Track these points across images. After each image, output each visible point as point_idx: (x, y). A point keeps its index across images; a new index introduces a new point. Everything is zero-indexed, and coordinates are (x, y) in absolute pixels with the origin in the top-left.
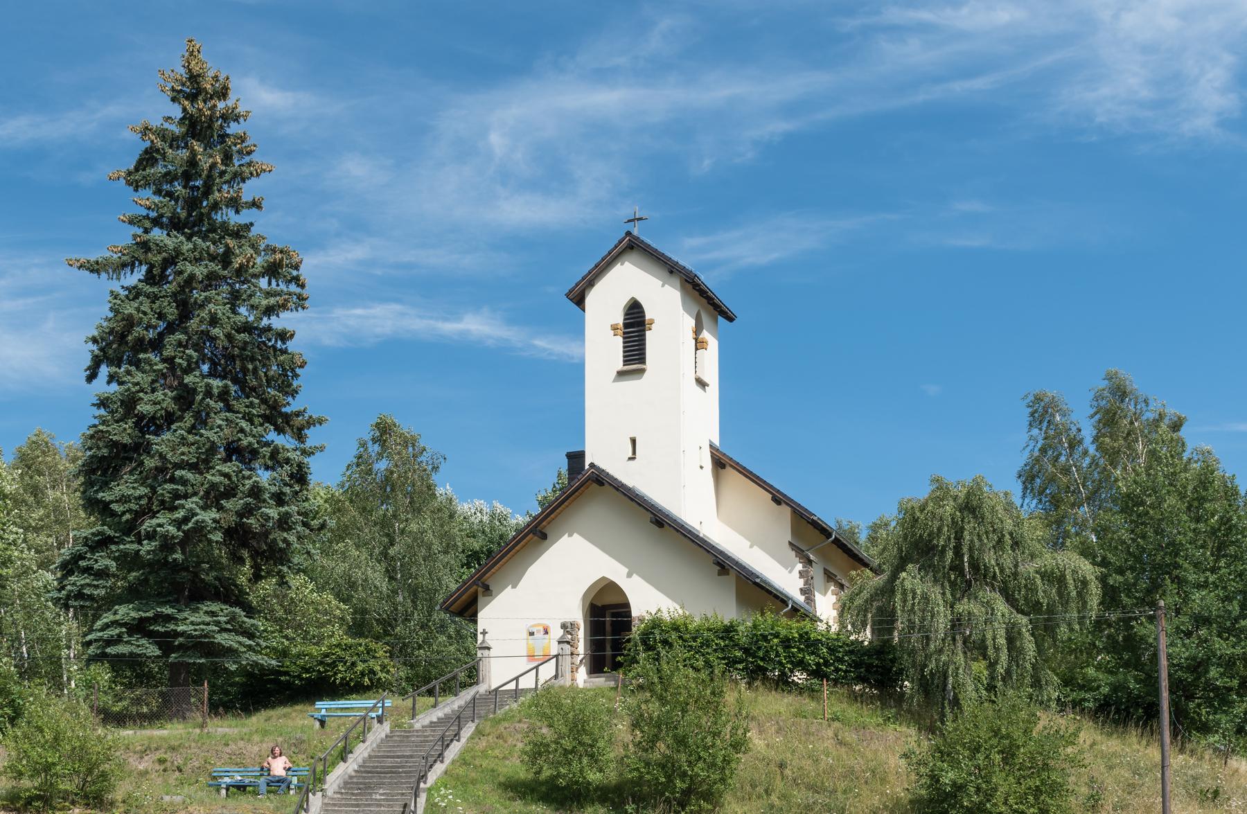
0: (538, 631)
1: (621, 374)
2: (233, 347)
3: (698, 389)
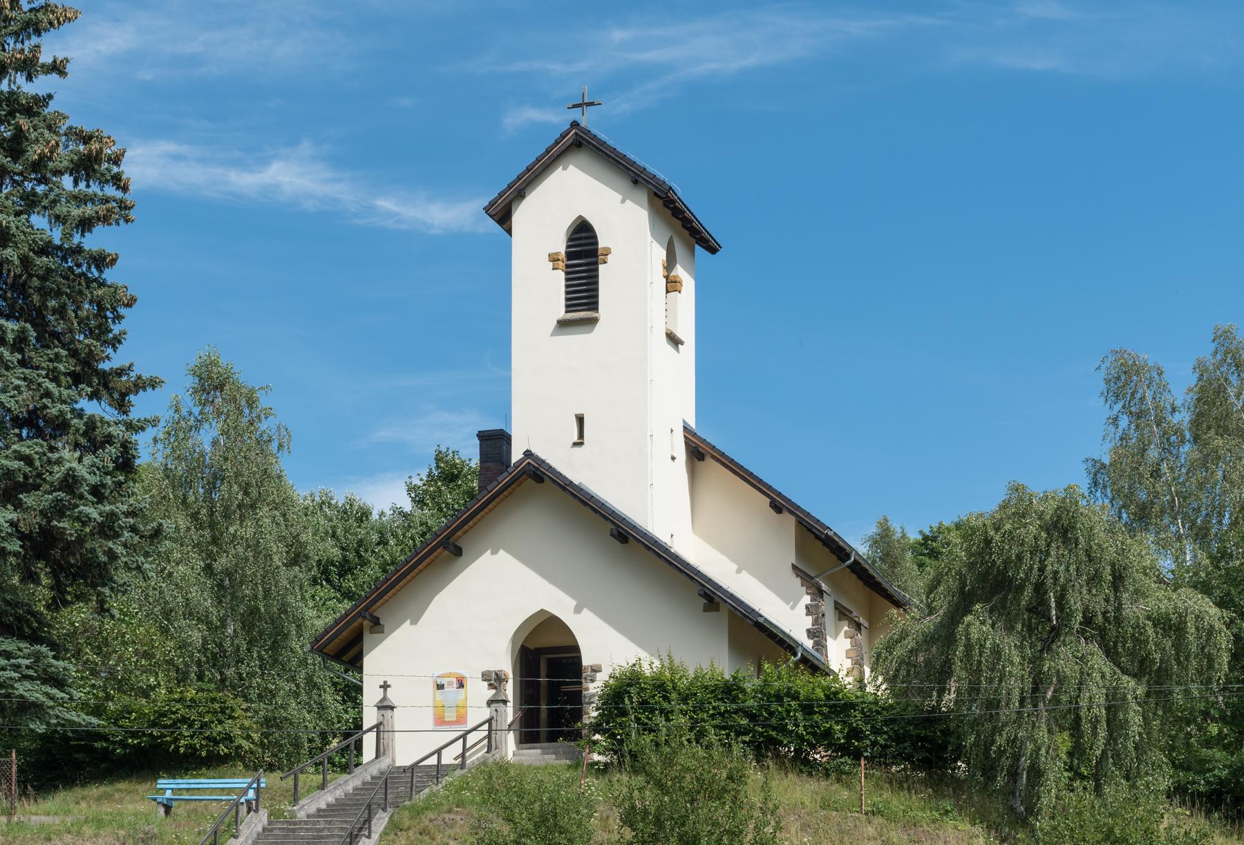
0: (450, 683)
1: (563, 324)
2: (31, 276)
3: (669, 348)
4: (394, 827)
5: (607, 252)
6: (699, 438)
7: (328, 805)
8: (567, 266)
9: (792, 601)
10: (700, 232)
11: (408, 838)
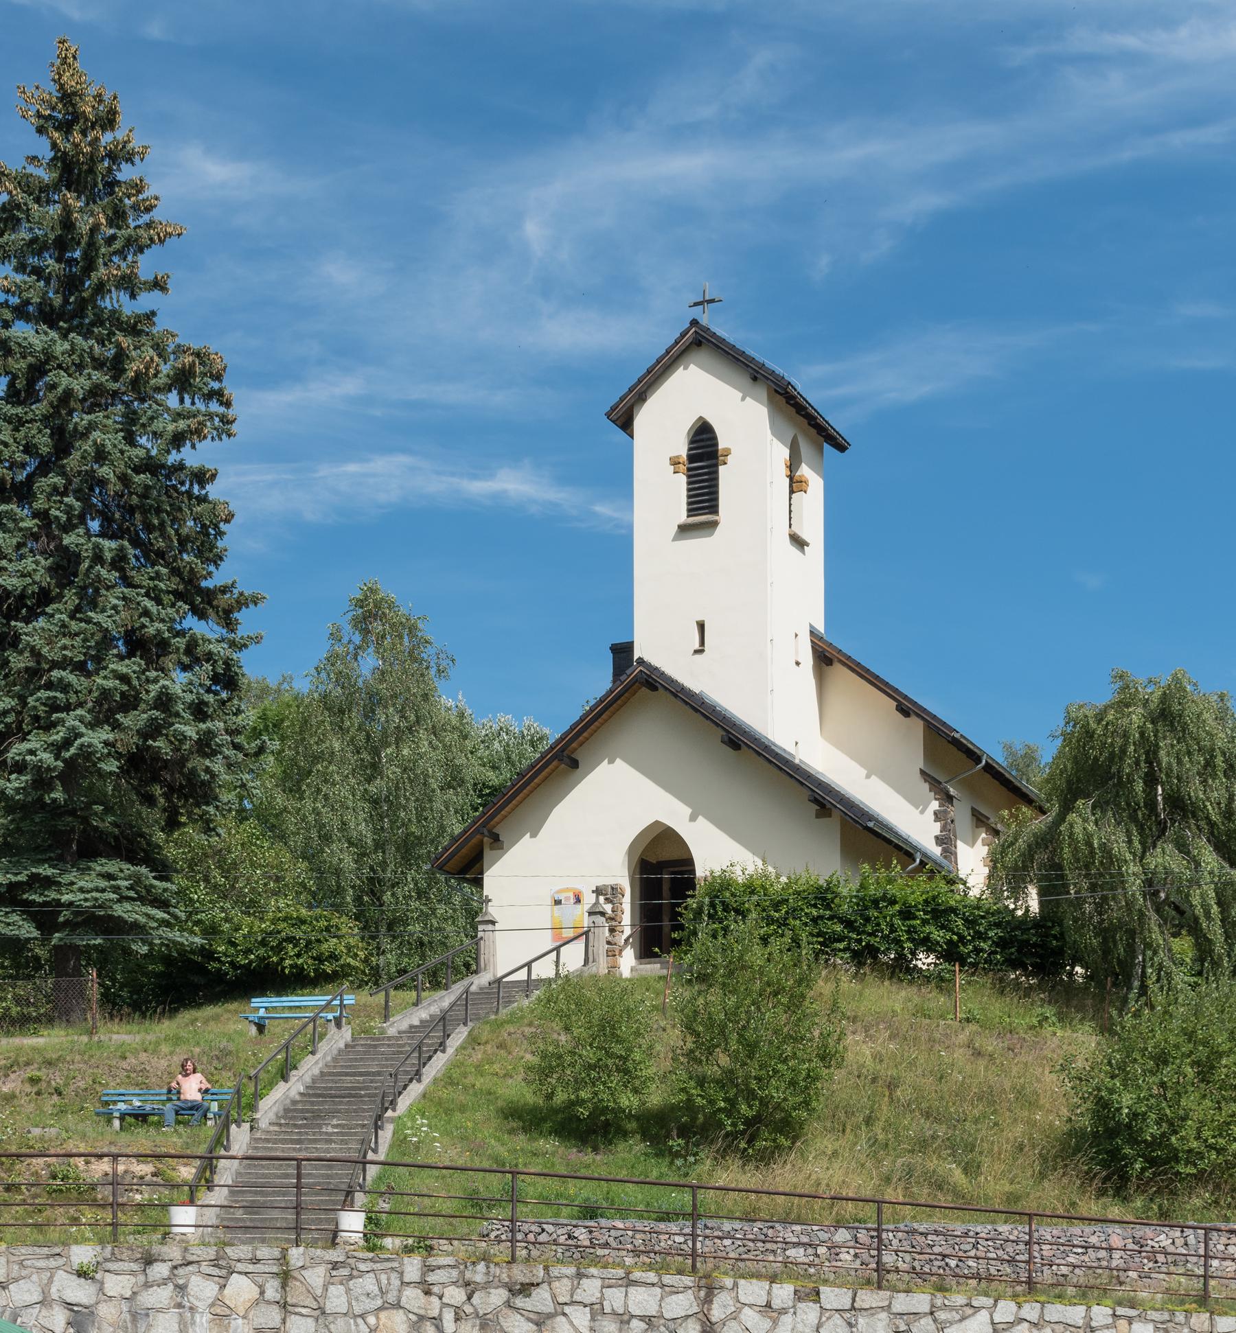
0: (567, 898)
1: (685, 530)
2: (131, 494)
3: (794, 551)
4: (473, 1041)
5: (727, 452)
6: (825, 642)
8: (689, 469)
9: (921, 805)
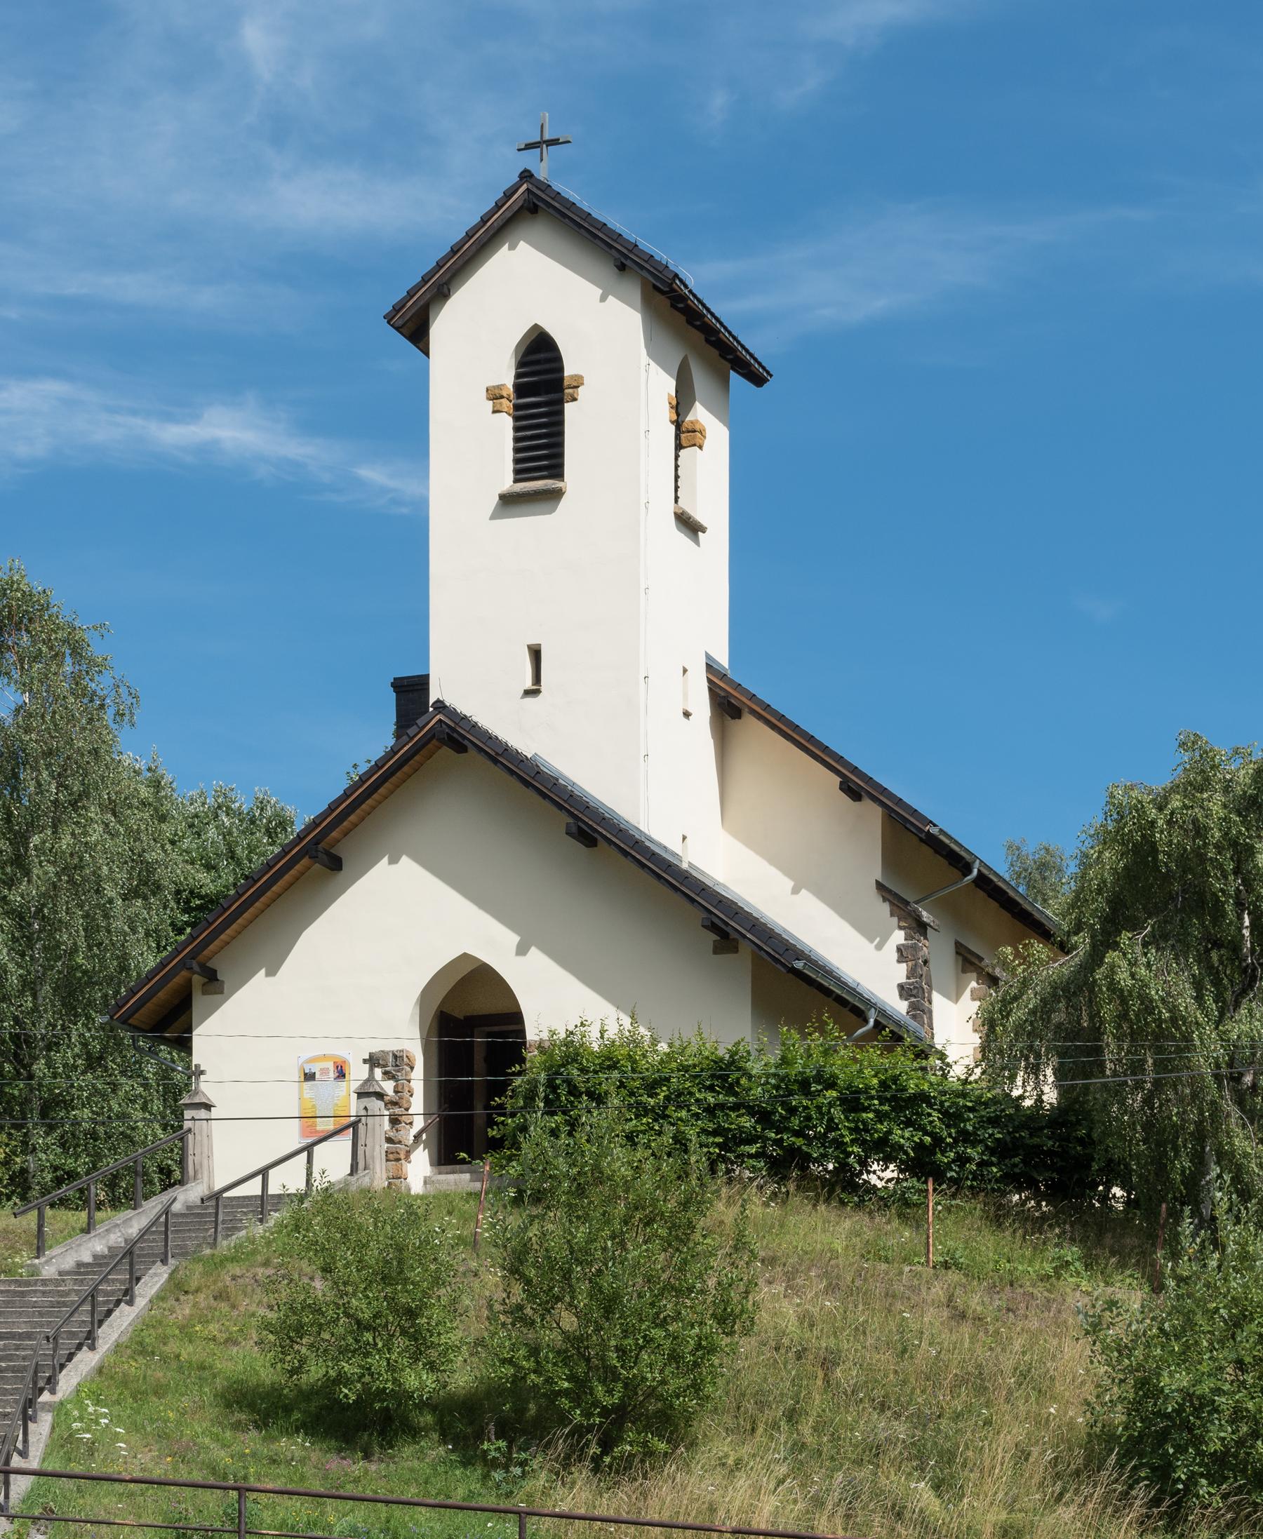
1: (509, 502)
3: (682, 539)
4: (177, 1287)
5: (578, 382)
6: (730, 682)
7: (95, 1257)
8: (517, 407)
9: (876, 936)
10: (734, 350)
11: (195, 1305)
